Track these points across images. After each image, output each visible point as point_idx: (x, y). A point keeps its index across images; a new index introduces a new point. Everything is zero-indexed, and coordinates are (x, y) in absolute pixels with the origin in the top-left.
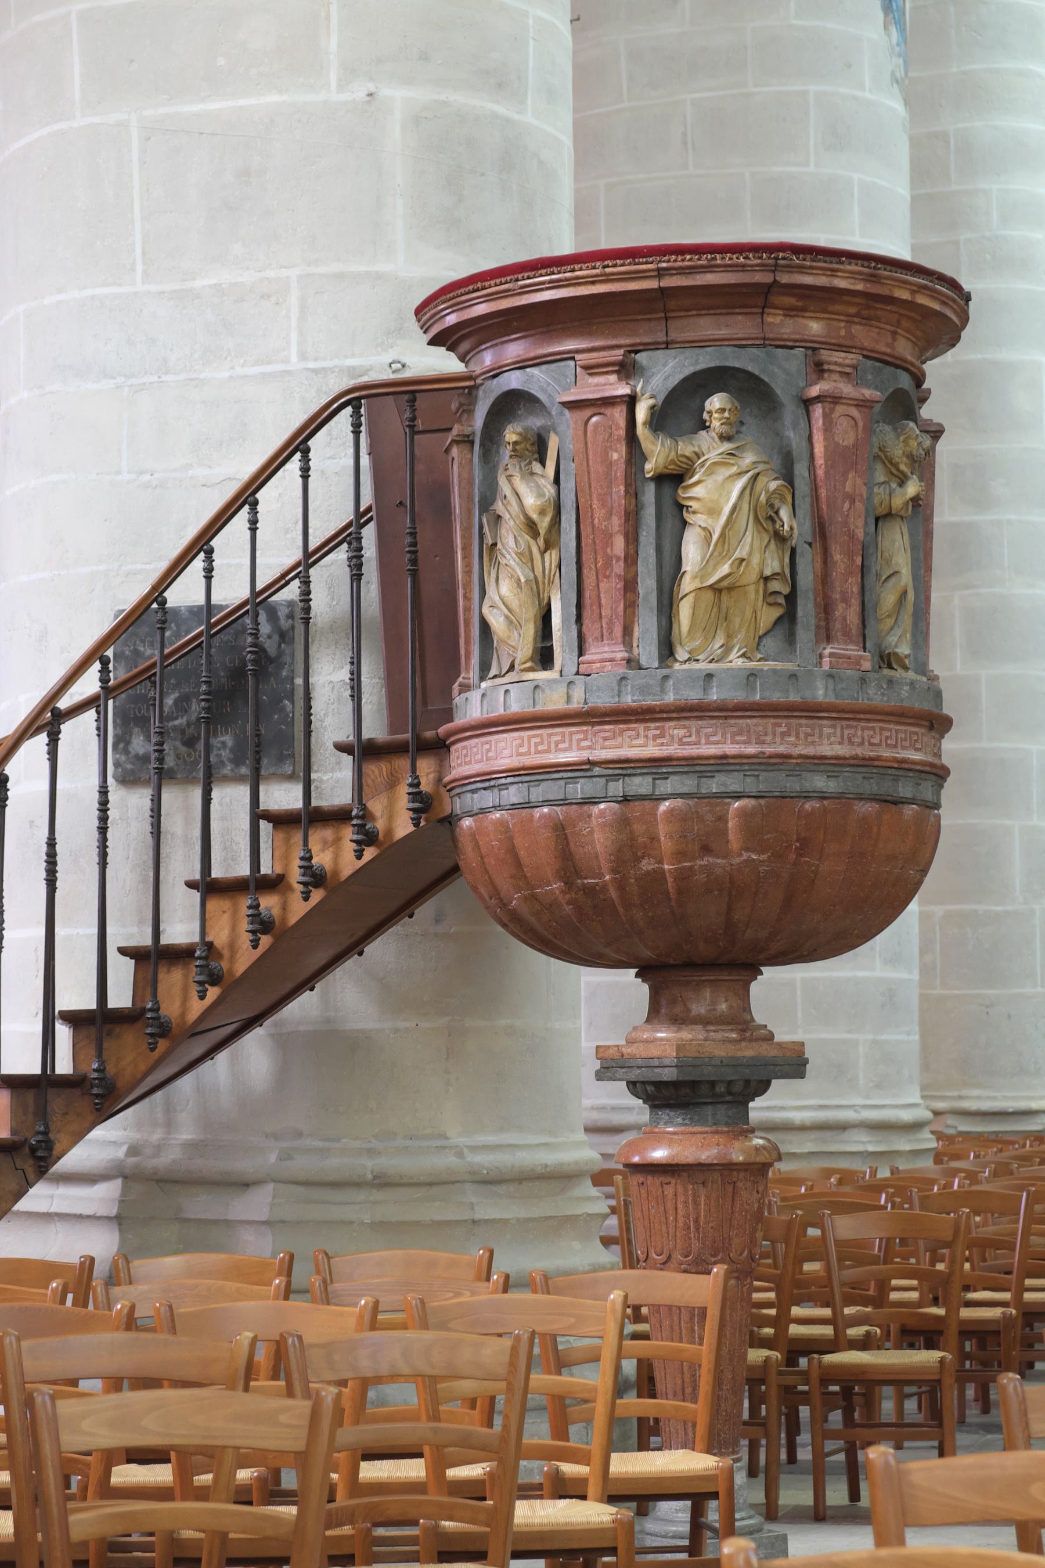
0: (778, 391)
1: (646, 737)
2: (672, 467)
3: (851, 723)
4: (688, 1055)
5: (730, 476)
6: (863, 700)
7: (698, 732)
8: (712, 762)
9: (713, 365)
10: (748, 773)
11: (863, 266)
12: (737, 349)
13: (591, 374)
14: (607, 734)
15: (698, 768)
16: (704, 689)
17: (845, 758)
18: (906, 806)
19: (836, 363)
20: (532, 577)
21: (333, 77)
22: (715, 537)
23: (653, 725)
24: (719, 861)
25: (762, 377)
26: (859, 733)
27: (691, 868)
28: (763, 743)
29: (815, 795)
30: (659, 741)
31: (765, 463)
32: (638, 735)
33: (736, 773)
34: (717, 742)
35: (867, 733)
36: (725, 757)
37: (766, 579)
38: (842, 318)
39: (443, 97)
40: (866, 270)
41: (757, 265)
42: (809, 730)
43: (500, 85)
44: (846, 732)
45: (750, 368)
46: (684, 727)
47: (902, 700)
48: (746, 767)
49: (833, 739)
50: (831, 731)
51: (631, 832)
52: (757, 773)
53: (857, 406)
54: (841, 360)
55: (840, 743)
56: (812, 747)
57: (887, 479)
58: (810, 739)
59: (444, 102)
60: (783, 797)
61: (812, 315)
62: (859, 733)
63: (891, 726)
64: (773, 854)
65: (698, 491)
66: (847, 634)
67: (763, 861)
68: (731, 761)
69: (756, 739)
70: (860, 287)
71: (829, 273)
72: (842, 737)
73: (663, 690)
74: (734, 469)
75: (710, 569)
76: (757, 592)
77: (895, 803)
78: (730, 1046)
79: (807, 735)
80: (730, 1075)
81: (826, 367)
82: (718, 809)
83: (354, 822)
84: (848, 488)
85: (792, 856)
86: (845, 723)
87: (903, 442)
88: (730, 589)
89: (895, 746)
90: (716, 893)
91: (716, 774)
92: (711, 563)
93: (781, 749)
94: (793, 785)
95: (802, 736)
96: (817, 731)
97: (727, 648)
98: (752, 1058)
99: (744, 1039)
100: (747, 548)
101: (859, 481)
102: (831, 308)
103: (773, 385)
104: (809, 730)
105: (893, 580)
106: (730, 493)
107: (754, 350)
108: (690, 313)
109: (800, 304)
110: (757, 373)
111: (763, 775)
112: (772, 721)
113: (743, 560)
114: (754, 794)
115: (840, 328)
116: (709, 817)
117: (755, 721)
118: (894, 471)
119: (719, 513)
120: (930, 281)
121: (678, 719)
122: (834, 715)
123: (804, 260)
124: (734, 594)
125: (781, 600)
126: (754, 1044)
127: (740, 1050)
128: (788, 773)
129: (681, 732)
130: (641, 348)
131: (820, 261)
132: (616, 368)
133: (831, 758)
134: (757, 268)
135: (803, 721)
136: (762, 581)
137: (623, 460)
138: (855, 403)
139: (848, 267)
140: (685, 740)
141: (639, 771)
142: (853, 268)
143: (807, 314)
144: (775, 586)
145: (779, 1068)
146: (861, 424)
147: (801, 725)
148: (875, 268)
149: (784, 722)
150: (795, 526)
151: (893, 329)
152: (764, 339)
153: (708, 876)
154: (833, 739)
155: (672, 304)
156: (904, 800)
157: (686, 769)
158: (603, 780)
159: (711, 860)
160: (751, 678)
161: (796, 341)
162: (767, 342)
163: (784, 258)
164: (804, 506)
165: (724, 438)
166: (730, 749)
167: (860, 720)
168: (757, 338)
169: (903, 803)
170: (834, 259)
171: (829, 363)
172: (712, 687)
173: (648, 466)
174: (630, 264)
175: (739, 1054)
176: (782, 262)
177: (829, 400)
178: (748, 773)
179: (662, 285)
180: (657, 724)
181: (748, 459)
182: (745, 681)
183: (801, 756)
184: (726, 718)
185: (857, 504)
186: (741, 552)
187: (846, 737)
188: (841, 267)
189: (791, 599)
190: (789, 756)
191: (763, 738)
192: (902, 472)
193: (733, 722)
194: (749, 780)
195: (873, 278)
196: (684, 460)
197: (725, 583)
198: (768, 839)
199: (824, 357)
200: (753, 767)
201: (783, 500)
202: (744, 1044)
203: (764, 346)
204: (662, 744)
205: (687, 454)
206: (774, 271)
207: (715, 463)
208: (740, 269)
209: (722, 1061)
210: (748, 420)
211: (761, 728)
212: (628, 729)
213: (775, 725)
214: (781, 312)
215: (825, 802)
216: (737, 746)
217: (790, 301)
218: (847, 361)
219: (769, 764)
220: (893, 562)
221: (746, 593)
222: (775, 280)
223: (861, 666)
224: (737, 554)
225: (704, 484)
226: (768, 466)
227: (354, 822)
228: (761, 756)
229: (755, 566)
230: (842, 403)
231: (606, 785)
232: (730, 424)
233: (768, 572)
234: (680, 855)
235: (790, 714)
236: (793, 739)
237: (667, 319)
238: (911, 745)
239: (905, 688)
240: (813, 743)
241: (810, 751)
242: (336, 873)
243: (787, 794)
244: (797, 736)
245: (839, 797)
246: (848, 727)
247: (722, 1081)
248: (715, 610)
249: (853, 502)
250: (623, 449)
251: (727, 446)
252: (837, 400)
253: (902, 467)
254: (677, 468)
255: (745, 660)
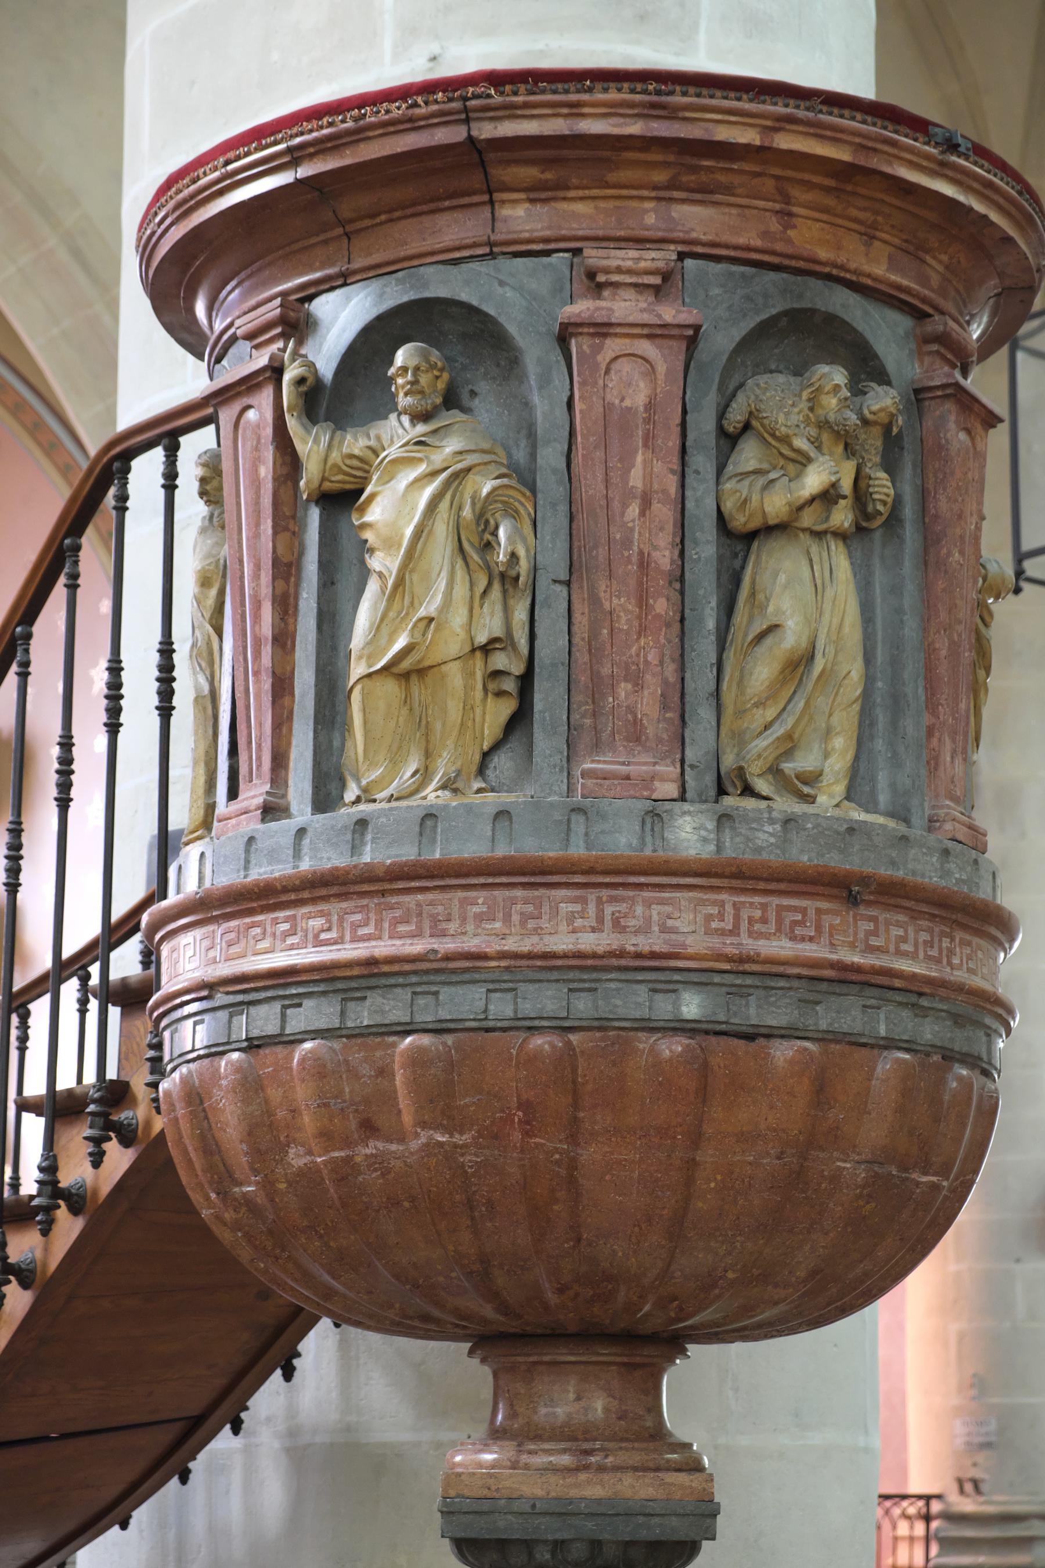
0: (512, 329)
1: (274, 935)
2: (340, 477)
3: (620, 892)
4: (467, 1492)
5: (417, 480)
6: (655, 851)
7: (341, 920)
8: (356, 972)
9: (405, 299)
10: (419, 989)
11: (633, 91)
12: (441, 267)
13: (256, 347)
14: (233, 935)
15: (340, 985)
16: (353, 847)
17: (594, 956)
18: (777, 1042)
19: (619, 270)
20: (206, 688)
21: (388, 44)
22: (390, 583)
23: (281, 914)
24: (394, 1147)
25: (485, 308)
26: (639, 910)
27: (348, 1160)
28: (443, 934)
29: (545, 1023)
30: (290, 941)
31: (484, 452)
32: (264, 933)
33: (399, 990)
34: (368, 938)
35: (655, 911)
36: (371, 962)
37: (487, 649)
38: (645, 193)
39: (540, 46)
40: (638, 97)
41: (433, 115)
42: (530, 908)
43: (642, 18)
44: (609, 910)
45: (464, 296)
46: (322, 914)
47: (759, 850)
48: (414, 979)
49: (579, 923)
50: (578, 907)
51: (267, 1101)
52: (434, 988)
53: (649, 336)
54: (629, 264)
55: (593, 930)
56: (535, 939)
57: (765, 466)
58: (531, 924)
59: (541, 51)
60: (487, 1030)
61: (580, 193)
62: (639, 910)
63: (724, 896)
64: (480, 1135)
65: (375, 514)
66: (636, 736)
67: (465, 1146)
68: (386, 968)
69: (431, 927)
70: (635, 128)
71: (565, 111)
72: (600, 920)
73: (297, 854)
74: (422, 468)
75: (383, 642)
76: (470, 675)
77: (750, 1037)
78: (553, 1479)
79: (525, 918)
80: (552, 1530)
81: (601, 278)
82: (378, 1054)
83: (92, 1108)
84: (636, 479)
85: (517, 1136)
86: (605, 893)
87: (809, 400)
88: (421, 672)
89: (735, 932)
90: (406, 1204)
91: (368, 993)
92: (385, 631)
93: (472, 943)
94: (501, 1008)
95: (516, 918)
96: (546, 908)
97: (424, 774)
98: (599, 1501)
99: (586, 1468)
100: (439, 598)
101: (658, 467)
102: (612, 177)
103: (502, 320)
104: (530, 908)
105: (769, 641)
106: (414, 509)
107: (475, 266)
108: (378, 220)
109: (548, 176)
110: (475, 303)
111: (445, 992)
112: (460, 894)
113: (431, 620)
114: (430, 1026)
115: (647, 211)
116: (366, 1070)
117: (430, 896)
118: (786, 451)
119: (400, 545)
120: (808, 109)
121: (314, 900)
122: (579, 879)
123: (515, 93)
124: (429, 679)
125: (510, 685)
126: (606, 1477)
127: (577, 1485)
128: (491, 986)
129: (317, 923)
130: (312, 290)
131: (543, 92)
132: (278, 330)
133: (565, 956)
134: (436, 121)
135: (519, 893)
136: (478, 654)
137: (270, 477)
138: (645, 331)
139: (600, 96)
140: (323, 936)
141: (263, 995)
142: (613, 96)
143: (572, 194)
144: (500, 661)
145: (656, 1520)
146: (661, 368)
147: (514, 901)
148: (658, 93)
149: (481, 896)
150: (521, 552)
151: (778, 207)
152: (491, 244)
153: (383, 1175)
154: (579, 923)
155: (346, 208)
156: (763, 1031)
157: (322, 988)
158: (223, 1015)
159: (380, 1145)
160: (429, 823)
161: (547, 240)
162: (495, 249)
163: (475, 97)
164: (554, 521)
165: (421, 416)
166: (383, 948)
167: (640, 886)
168: (474, 245)
169: (768, 1036)
170: (572, 86)
171: (607, 271)
172: (365, 844)
173: (302, 483)
174: (256, 150)
175: (574, 1493)
176: (473, 103)
177: (586, 330)
178: (419, 989)
179: (299, 176)
180: (288, 913)
181: (451, 445)
182: (417, 829)
183: (503, 955)
184: (383, 893)
185: (656, 506)
186: (430, 607)
187: (608, 918)
188: (585, 97)
189: (526, 680)
190: (483, 957)
191: (444, 925)
192: (798, 451)
193: (394, 900)
194: (421, 1001)
195: (656, 110)
196: (355, 463)
197: (406, 665)
198: (467, 1106)
199: (591, 262)
200: (425, 978)
201: (513, 513)
202: (583, 1476)
203: (492, 255)
204: (292, 947)
205: (356, 452)
206: (467, 121)
207: (394, 462)
208: (408, 126)
209: (534, 1506)
210: (483, 387)
211: (440, 908)
212: (253, 925)
213: (463, 902)
214: (522, 196)
215: (574, 1038)
216: (398, 942)
217: (530, 173)
218: (643, 264)
219: (454, 971)
220: (771, 609)
221: (443, 677)
222: (470, 138)
223: (653, 791)
224: (422, 612)
225: (379, 499)
226: (487, 458)
227: (92, 1108)
228: (432, 957)
229: (459, 630)
230: (616, 335)
231: (230, 1022)
232: (422, 392)
233: (482, 639)
234: (327, 1137)
235: (490, 880)
236: (498, 925)
237: (347, 235)
238: (779, 929)
239: (769, 829)
240: (537, 931)
241: (526, 946)
242: (95, 1192)
243: (491, 1024)
244: (507, 919)
245: (601, 1025)
246: (613, 899)
247: (545, 1542)
248: (405, 711)
249: (646, 503)
250: (269, 453)
251: (421, 428)
252: (604, 330)
253: (800, 443)
254: (347, 478)
255: (447, 793)
